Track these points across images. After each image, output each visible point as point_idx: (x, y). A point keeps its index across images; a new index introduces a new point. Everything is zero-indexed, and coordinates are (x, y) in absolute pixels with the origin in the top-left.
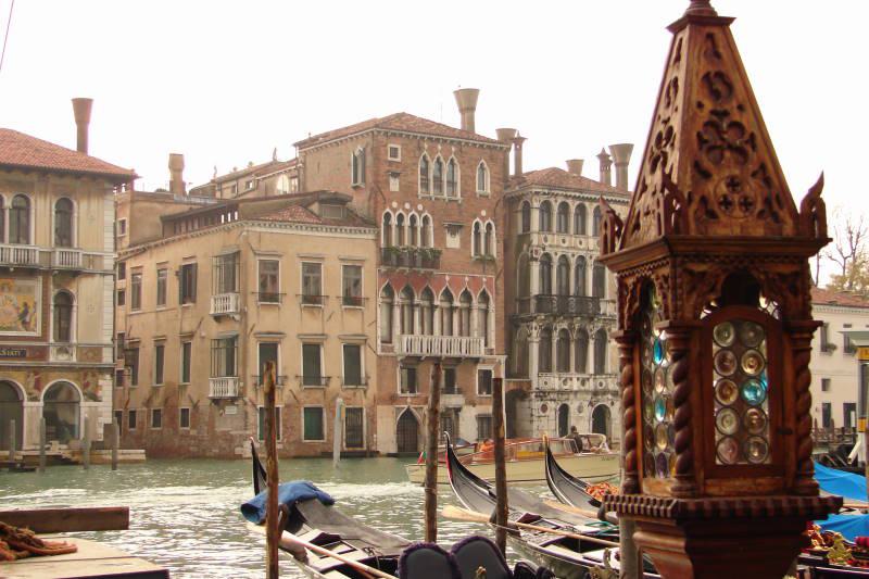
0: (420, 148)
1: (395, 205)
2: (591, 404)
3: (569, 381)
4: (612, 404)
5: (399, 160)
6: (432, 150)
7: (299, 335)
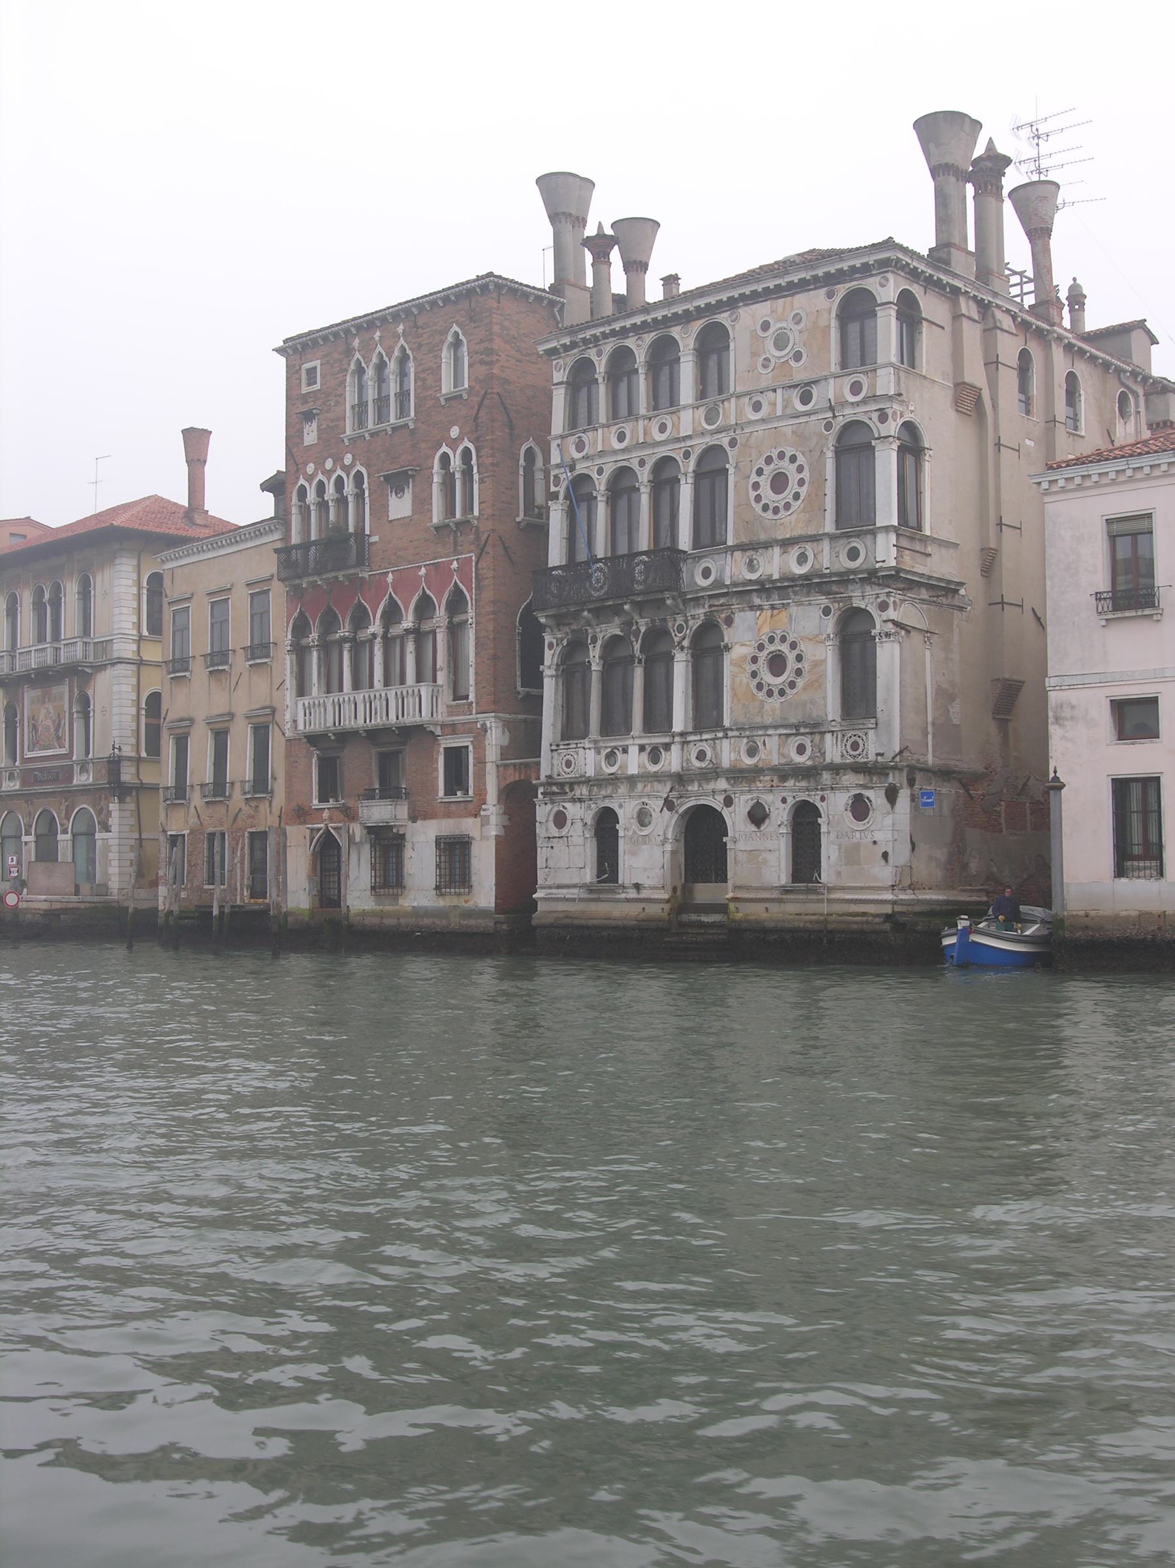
0: (349, 352)
1: (310, 468)
2: (669, 805)
3: (619, 755)
4: (728, 802)
5: (317, 387)
6: (367, 348)
7: (207, 718)
